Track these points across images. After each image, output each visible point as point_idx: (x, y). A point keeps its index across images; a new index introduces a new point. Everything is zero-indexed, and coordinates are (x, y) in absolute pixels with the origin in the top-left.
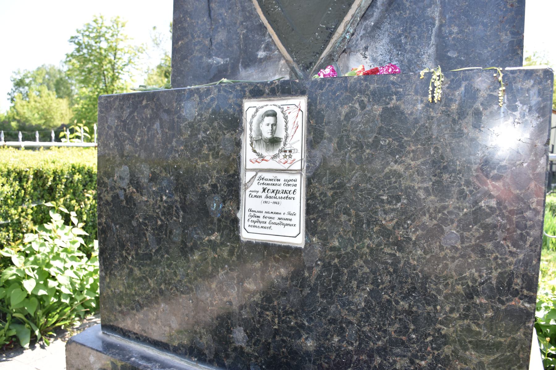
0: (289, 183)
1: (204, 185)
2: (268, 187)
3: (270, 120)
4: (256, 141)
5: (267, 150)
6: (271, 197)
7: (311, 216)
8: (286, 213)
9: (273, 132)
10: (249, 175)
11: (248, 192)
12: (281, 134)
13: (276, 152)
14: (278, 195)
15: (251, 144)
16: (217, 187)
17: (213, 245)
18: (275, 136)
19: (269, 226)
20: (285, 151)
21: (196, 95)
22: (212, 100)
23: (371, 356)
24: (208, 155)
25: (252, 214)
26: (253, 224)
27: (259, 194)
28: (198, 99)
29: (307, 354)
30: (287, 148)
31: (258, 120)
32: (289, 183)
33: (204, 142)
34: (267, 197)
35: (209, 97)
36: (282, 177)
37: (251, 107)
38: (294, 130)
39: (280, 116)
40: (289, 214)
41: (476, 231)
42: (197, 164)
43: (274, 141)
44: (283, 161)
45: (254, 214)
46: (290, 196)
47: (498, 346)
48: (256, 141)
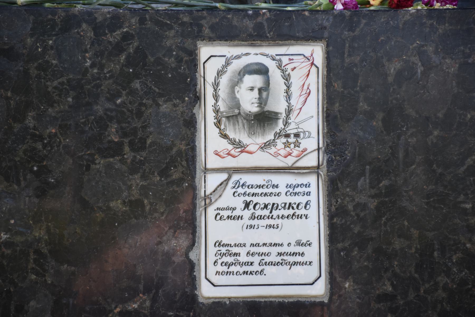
0: (297, 190)
1: (112, 204)
2: (255, 199)
3: (255, 80)
4: (228, 118)
5: (252, 133)
6: (261, 218)
7: (340, 245)
8: (293, 243)
9: (262, 102)
10: (213, 181)
11: (211, 211)
12: (278, 105)
13: (270, 136)
14: (275, 213)
15: (218, 124)
16: (143, 206)
18: (267, 108)
19: (259, 269)
20: (287, 136)
21: (84, 26)
22: (126, 37)
24: (120, 145)
25: (224, 250)
26: (225, 269)
27: (236, 213)
28: (91, 34)
30: (291, 129)
31: (231, 80)
32: (297, 190)
33: (111, 119)
34: (253, 217)
35: (118, 32)
36: (282, 180)
38: (302, 99)
39: (275, 74)
40: (299, 243)
42: (93, 162)
44: (283, 152)
46: (298, 212)
48: (228, 118)
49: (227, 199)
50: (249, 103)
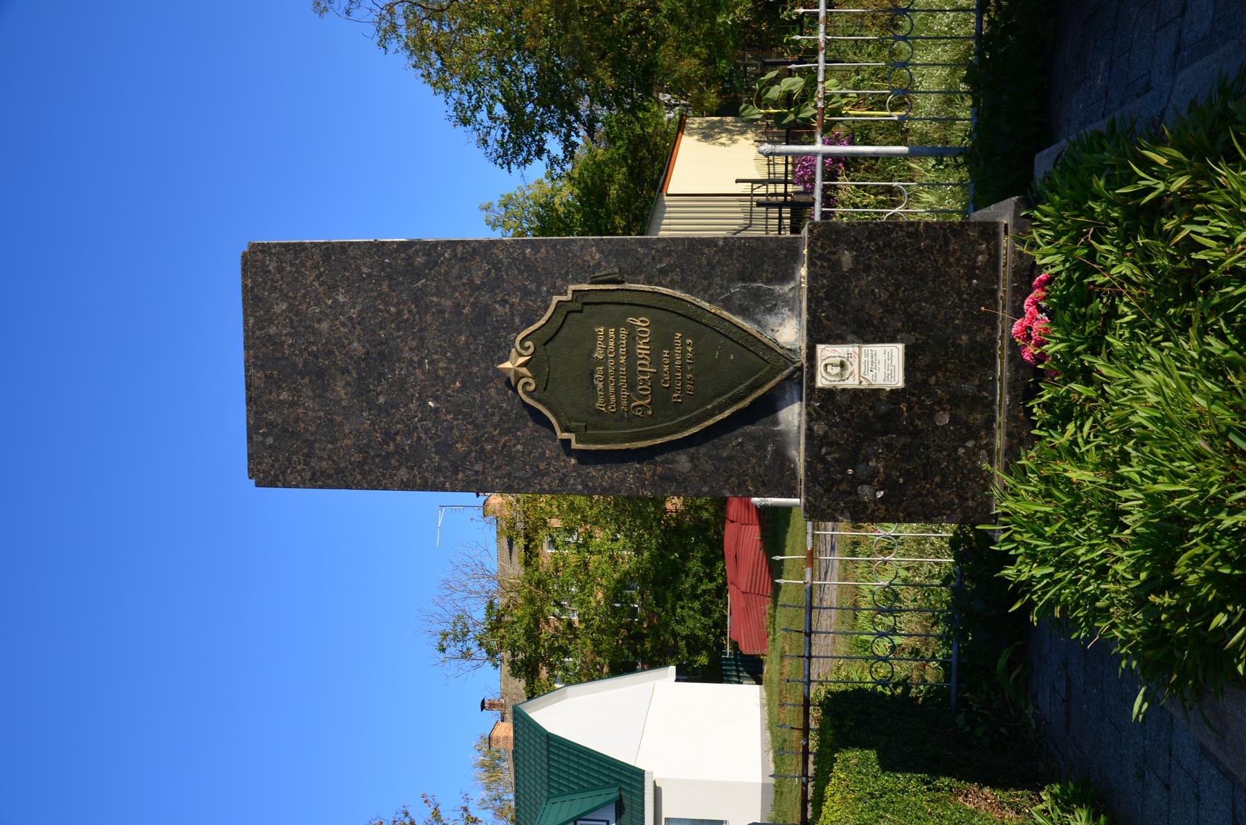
3: (829, 368)
12: (838, 360)
17: (910, 409)
23: (964, 300)
29: (970, 339)
37: (822, 381)
41: (887, 251)
43: (842, 365)
45: (887, 377)
47: (945, 236)
49: (870, 378)
50: (838, 370)
